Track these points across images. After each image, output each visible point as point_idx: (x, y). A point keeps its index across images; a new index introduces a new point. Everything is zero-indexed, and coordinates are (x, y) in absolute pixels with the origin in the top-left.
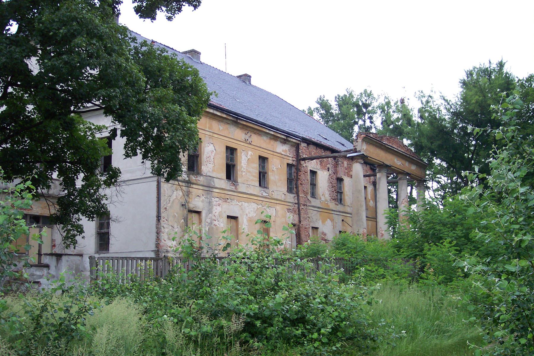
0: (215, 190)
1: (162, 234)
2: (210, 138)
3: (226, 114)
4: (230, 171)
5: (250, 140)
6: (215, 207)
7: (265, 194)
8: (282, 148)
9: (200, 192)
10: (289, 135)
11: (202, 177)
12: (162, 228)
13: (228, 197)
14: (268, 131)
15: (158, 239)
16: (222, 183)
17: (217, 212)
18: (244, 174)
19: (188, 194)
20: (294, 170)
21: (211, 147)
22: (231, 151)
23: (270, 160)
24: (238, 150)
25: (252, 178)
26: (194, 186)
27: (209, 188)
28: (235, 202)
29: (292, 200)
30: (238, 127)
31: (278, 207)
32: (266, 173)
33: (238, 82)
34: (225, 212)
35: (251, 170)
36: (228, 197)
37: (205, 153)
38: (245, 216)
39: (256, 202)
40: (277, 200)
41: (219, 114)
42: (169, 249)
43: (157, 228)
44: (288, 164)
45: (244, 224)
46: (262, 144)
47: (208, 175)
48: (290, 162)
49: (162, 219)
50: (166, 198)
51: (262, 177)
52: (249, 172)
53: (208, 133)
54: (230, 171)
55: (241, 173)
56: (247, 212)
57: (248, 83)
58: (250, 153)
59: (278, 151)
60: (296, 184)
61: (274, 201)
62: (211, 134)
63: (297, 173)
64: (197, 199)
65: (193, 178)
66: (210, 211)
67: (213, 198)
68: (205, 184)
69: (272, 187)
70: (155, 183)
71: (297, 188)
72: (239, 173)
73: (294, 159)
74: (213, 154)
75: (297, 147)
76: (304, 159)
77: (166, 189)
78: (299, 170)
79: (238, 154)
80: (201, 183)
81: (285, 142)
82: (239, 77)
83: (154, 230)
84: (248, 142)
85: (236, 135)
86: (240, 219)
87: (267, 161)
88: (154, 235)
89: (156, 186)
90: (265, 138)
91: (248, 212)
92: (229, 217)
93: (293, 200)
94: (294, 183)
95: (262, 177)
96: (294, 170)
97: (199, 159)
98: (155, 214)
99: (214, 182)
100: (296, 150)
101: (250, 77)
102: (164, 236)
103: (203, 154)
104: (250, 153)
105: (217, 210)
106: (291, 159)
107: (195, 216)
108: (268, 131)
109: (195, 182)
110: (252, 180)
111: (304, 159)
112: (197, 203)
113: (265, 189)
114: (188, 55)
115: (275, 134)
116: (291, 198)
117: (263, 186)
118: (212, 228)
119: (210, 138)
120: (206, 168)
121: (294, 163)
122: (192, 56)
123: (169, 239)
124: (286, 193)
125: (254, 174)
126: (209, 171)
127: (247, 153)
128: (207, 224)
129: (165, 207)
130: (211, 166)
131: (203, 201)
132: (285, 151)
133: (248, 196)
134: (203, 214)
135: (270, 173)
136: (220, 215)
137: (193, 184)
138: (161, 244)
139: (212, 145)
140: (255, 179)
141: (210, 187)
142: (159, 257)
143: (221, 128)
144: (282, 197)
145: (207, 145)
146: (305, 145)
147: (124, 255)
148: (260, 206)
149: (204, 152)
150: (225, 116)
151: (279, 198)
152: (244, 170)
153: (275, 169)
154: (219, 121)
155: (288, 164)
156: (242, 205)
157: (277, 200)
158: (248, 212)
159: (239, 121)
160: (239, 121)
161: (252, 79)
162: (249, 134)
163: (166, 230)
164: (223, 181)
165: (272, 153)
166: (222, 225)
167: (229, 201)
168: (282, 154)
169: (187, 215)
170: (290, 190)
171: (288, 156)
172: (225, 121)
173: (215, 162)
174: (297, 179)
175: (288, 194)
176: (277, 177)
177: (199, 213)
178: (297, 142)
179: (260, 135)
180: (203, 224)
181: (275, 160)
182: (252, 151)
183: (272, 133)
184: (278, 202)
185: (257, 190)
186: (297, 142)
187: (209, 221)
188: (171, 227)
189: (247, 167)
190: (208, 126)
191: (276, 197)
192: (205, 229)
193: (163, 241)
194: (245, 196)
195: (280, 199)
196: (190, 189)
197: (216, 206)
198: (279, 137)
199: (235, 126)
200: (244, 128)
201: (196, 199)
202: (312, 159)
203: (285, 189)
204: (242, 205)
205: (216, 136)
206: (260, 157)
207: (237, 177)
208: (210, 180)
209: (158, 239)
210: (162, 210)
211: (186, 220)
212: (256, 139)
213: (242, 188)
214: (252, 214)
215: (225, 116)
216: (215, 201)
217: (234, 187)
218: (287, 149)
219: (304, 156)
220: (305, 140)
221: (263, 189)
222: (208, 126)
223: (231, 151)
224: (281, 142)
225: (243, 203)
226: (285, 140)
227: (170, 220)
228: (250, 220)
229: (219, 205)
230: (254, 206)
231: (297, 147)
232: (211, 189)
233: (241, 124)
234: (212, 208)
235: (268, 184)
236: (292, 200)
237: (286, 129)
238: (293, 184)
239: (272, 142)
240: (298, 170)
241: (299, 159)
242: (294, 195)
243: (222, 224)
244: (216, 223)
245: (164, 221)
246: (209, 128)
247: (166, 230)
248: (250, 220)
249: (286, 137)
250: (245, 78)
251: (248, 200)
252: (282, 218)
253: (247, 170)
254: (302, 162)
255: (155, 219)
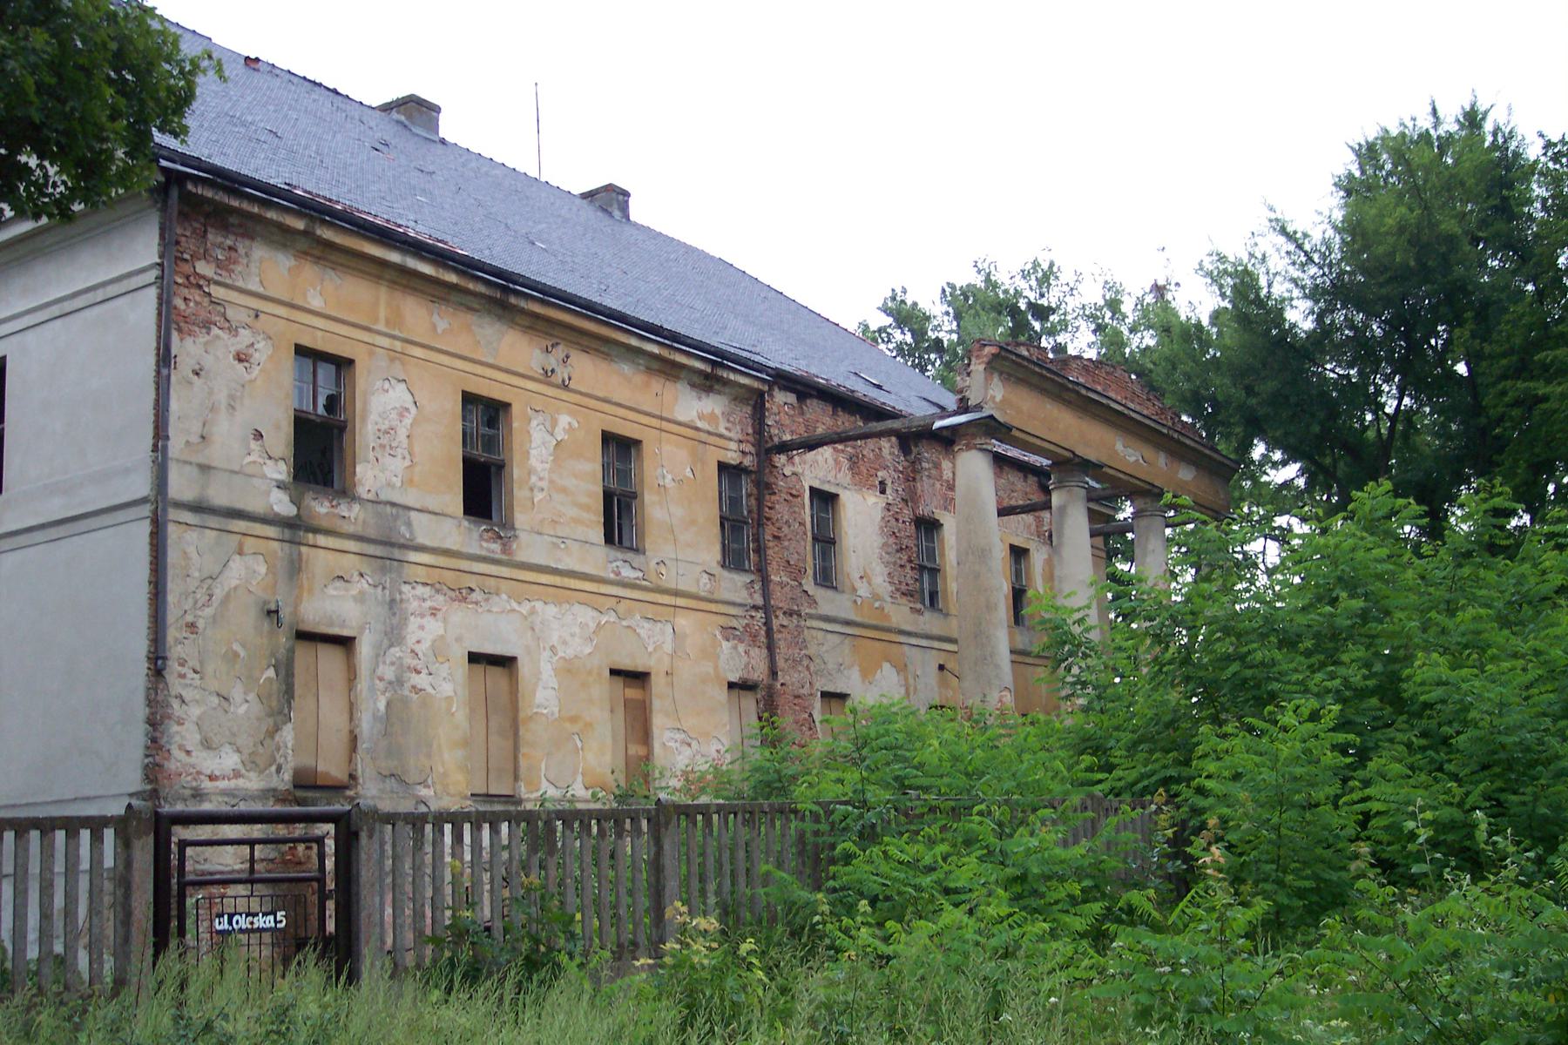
0: (414, 556)
1: (175, 728)
2: (392, 360)
3: (455, 270)
4: (483, 489)
5: (562, 373)
6: (414, 623)
7: (628, 573)
8: (693, 407)
9: (349, 563)
10: (721, 358)
11: (356, 507)
12: (176, 704)
13: (472, 582)
14: (634, 342)
15: (155, 743)
16: (441, 521)
17: (431, 639)
18: (539, 496)
19: (295, 568)
20: (746, 486)
21: (398, 395)
22: (486, 415)
23: (647, 448)
24: (515, 409)
25: (573, 512)
26: (321, 540)
27: (387, 548)
28: (501, 602)
29: (742, 596)
30: (513, 323)
31: (684, 622)
32: (634, 496)
33: (588, 212)
34: (459, 639)
35: (570, 483)
36: (472, 582)
37: (373, 417)
38: (548, 653)
39: (592, 601)
40: (677, 593)
41: (426, 269)
42: (207, 785)
43: (151, 702)
44: (723, 467)
45: (543, 690)
46: (620, 389)
47: (383, 497)
48: (732, 458)
49: (173, 668)
50: (192, 584)
51: (619, 516)
52: (564, 490)
53: (385, 342)
54: (483, 489)
55: (527, 493)
56: (555, 640)
57: (617, 214)
58: (564, 420)
59: (681, 418)
60: (757, 540)
61: (666, 598)
62: (398, 345)
63: (760, 501)
64: (334, 590)
65: (321, 508)
66: (394, 635)
67: (406, 588)
68: (371, 533)
69: (657, 547)
70: (145, 528)
71: (760, 550)
72: (520, 494)
73: (748, 448)
74: (408, 421)
75: (757, 403)
76: (784, 448)
77: (191, 550)
78: (768, 486)
79: (515, 425)
80: (351, 529)
81: (708, 383)
82: (589, 196)
83: (141, 712)
84: (557, 379)
85: (505, 356)
86: (524, 668)
87: (639, 451)
88: (138, 735)
89: (147, 539)
90: (626, 368)
91: (560, 642)
92: (474, 658)
93: (744, 593)
94: (748, 532)
95: (619, 516)
96: (746, 486)
97: (346, 437)
98: (140, 646)
99: (409, 524)
100: (753, 416)
101: (626, 194)
102: (183, 734)
103: (364, 419)
104: (564, 420)
105: (423, 632)
106: (733, 446)
107: (329, 657)
108: (634, 342)
109: (325, 524)
110: (577, 521)
111: (784, 448)
112: (334, 606)
113: (629, 556)
114: (395, 115)
115: (665, 353)
116: (736, 586)
117: (626, 543)
118: (405, 701)
119: (392, 360)
120: (373, 473)
121: (748, 461)
122: (409, 117)
123: (207, 744)
124: (717, 570)
125: (584, 500)
126: (390, 485)
127: (554, 423)
128: (380, 685)
129: (189, 618)
130: (397, 465)
131: (361, 598)
132: (712, 418)
133: (557, 580)
134: (364, 649)
135: (649, 498)
136: (439, 649)
137: (316, 531)
138: (172, 766)
139: (403, 386)
140: (585, 515)
141: (392, 545)
142: (157, 825)
143: (442, 325)
144: (703, 586)
145: (379, 384)
146: (791, 398)
147: (41, 813)
148: (612, 617)
149: (365, 411)
150: (452, 278)
151: (682, 586)
152: (544, 484)
153: (668, 481)
154: (435, 299)
155: (723, 467)
156: (533, 612)
157: (677, 593)
158: (560, 642)
159: (513, 300)
160: (513, 300)
161: (631, 201)
162: (560, 351)
163: (195, 711)
164: (448, 524)
165: (655, 422)
166: (447, 689)
167: (474, 596)
168: (697, 429)
169: (291, 651)
170: (732, 559)
171: (721, 436)
172: (455, 297)
173: (417, 449)
174: (761, 521)
175: (726, 573)
176: (678, 512)
177: (345, 643)
178: (756, 384)
179: (607, 356)
180: (363, 685)
181: (666, 448)
182: (570, 413)
183: (655, 349)
184: (681, 602)
185: (596, 557)
186: (756, 384)
187: (389, 673)
188: (215, 700)
189: (551, 471)
190: (382, 312)
191: (672, 585)
192: (373, 704)
193: (176, 752)
194: (544, 578)
195: (693, 590)
196: (304, 549)
197: (422, 616)
198: (682, 366)
199: (500, 318)
200: (538, 326)
201: (331, 591)
202: (811, 445)
203: (711, 554)
204: (533, 612)
205: (418, 352)
206: (608, 438)
207: (511, 507)
208: (396, 518)
209: (155, 743)
210: (172, 634)
211: (286, 670)
212: (586, 370)
213: (530, 548)
214: (578, 648)
215: (452, 278)
216: (415, 597)
217: (496, 547)
218: (718, 411)
219: (787, 437)
220: (784, 380)
221: (619, 555)
222: (382, 312)
223: (486, 415)
224: (693, 386)
225: (539, 605)
226: (706, 376)
227: (209, 669)
228: (568, 669)
229: (434, 612)
230: (586, 615)
231: (757, 403)
232: (397, 554)
233: (523, 311)
234: (404, 622)
235: (641, 536)
236: (742, 596)
237: (714, 341)
238: (743, 531)
239: (657, 384)
240: (764, 487)
241: (768, 449)
242: (747, 578)
243: (448, 684)
244: (421, 681)
245: (183, 676)
246: (388, 323)
247: (195, 711)
248: (568, 669)
249: (713, 369)
250: (611, 199)
251: (561, 595)
252: (694, 655)
253: (551, 482)
254: (780, 460)
255: (143, 666)
